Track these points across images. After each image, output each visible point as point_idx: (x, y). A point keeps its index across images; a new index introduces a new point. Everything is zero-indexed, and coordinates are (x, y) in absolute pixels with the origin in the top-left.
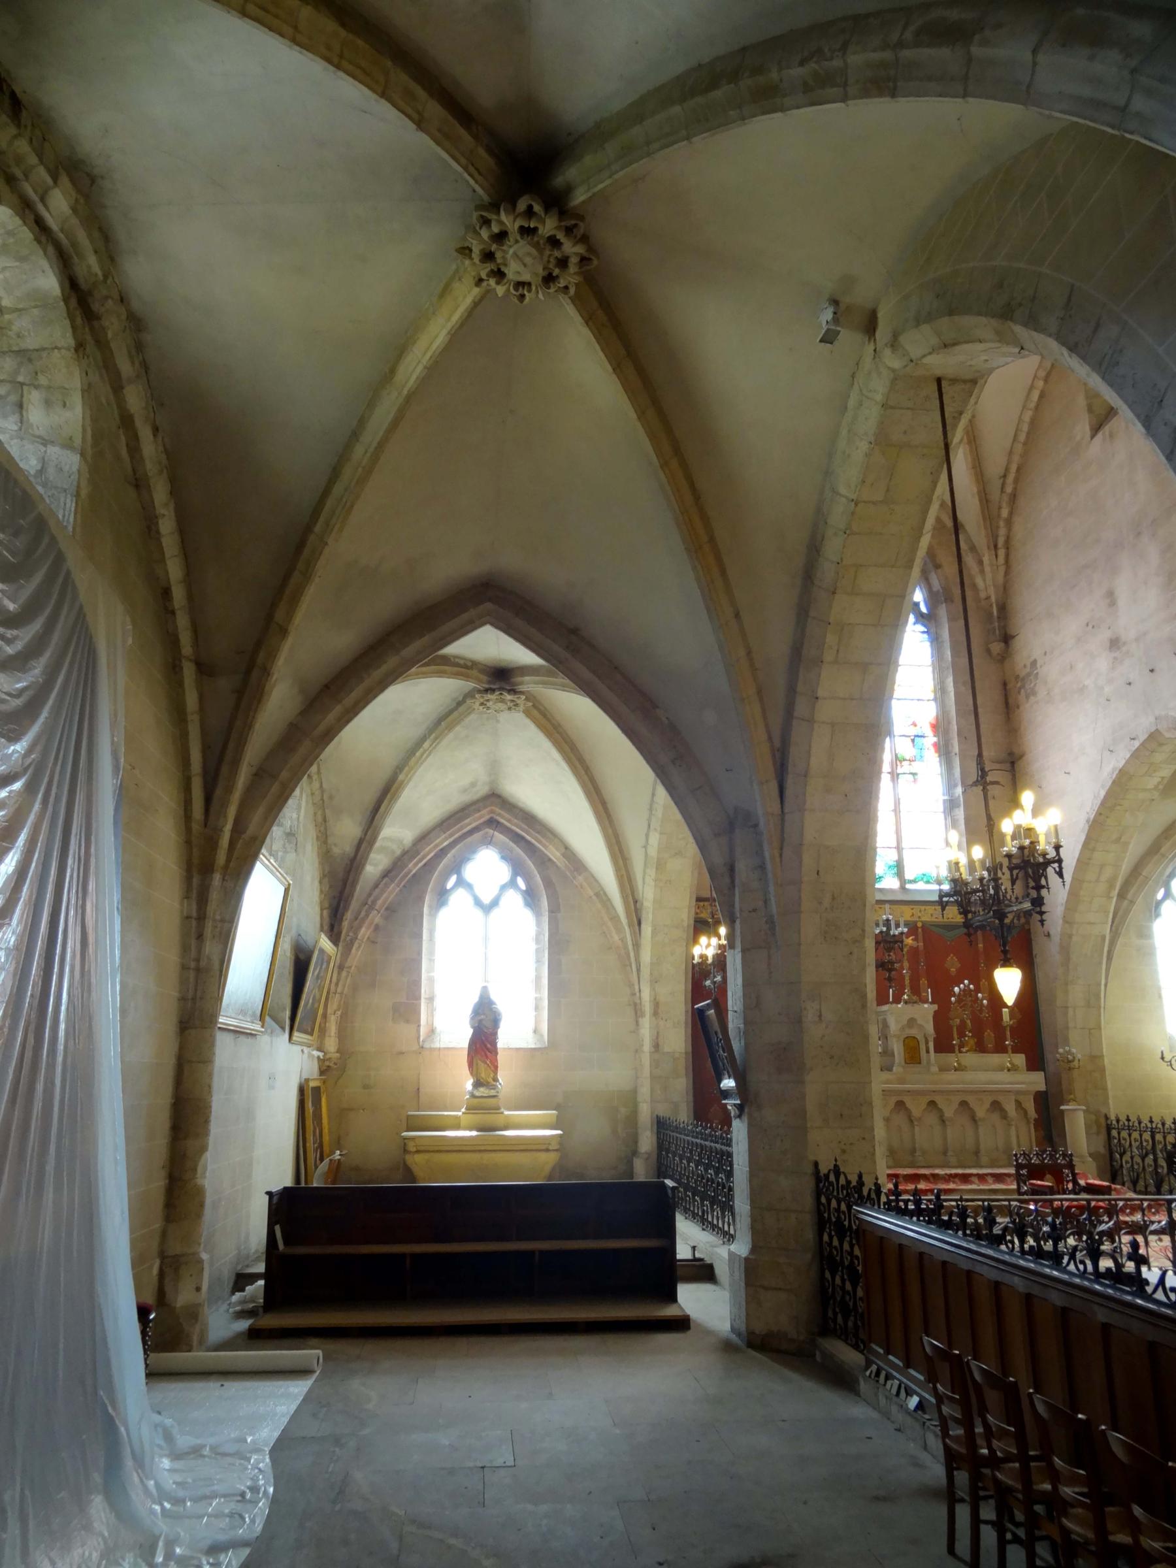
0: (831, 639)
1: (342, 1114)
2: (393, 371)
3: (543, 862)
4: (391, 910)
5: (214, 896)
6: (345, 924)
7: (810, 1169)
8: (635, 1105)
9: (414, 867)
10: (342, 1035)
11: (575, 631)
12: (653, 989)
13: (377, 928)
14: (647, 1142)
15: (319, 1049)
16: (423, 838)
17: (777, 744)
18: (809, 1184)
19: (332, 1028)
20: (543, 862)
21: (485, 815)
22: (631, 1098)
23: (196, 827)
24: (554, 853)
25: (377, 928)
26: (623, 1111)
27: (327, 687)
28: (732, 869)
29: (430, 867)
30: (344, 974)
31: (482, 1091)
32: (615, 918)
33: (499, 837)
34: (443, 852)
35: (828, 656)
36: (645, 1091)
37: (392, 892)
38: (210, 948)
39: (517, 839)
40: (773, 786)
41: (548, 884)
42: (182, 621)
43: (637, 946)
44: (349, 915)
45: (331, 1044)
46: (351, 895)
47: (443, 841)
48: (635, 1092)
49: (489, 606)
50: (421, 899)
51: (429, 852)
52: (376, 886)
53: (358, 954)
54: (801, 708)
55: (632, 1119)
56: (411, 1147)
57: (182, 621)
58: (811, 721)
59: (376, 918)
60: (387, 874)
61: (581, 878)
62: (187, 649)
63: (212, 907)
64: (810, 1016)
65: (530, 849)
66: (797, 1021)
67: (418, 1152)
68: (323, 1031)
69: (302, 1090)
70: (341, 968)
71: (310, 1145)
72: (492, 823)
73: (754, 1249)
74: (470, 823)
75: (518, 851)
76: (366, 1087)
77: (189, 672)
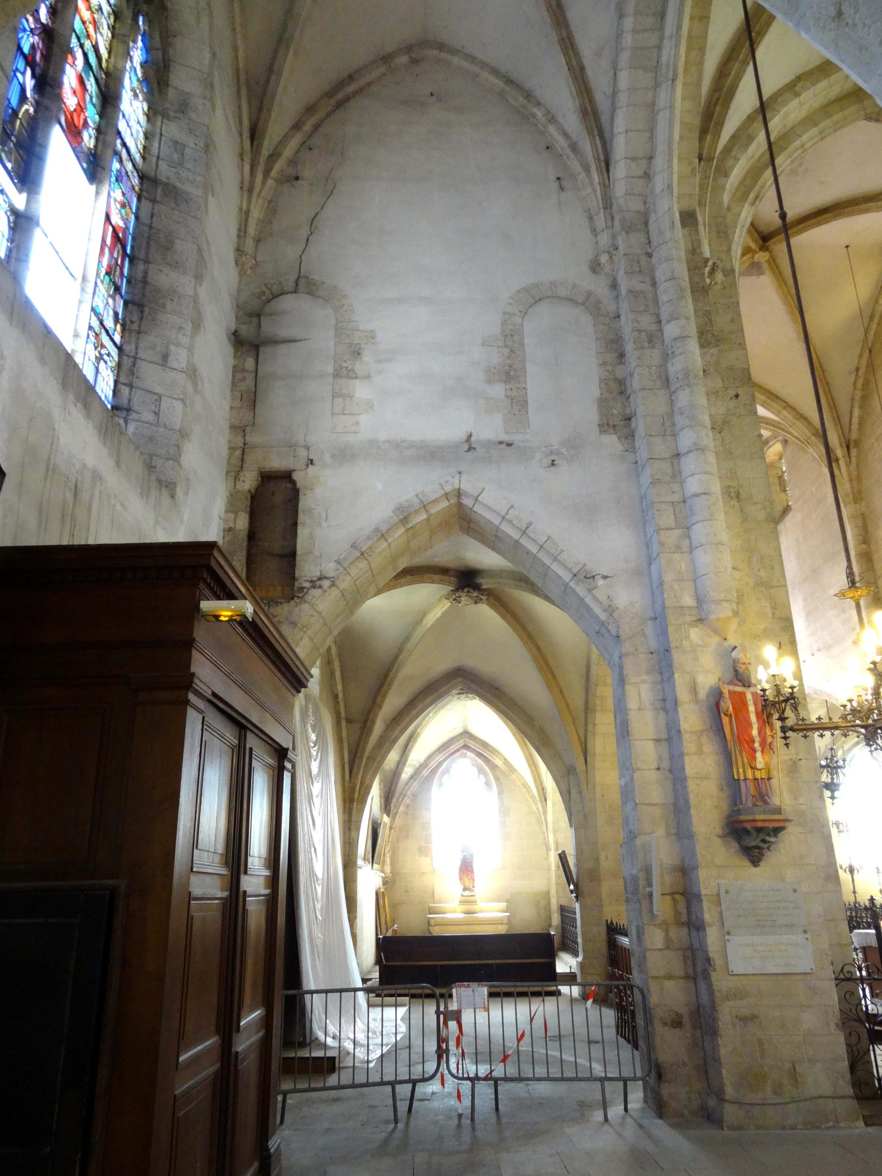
0: (598, 702)
1: (394, 906)
2: (422, 620)
3: (493, 767)
4: (415, 796)
5: (354, 812)
6: (392, 805)
7: (605, 923)
8: (549, 899)
9: (425, 773)
10: (392, 865)
11: (497, 689)
12: (555, 835)
13: (408, 806)
14: (556, 920)
15: (382, 872)
16: (430, 757)
17: (583, 740)
18: (604, 929)
19: (388, 861)
20: (493, 767)
21: (461, 743)
23: (347, 784)
24: (498, 762)
25: (408, 806)
26: (543, 903)
27: (394, 719)
28: (570, 793)
29: (434, 771)
30: (392, 831)
31: (467, 893)
32: (533, 797)
33: (469, 754)
34: (441, 763)
35: (598, 708)
36: (553, 891)
37: (415, 785)
38: (353, 834)
39: (479, 755)
40: (583, 758)
41: (497, 779)
42: (342, 705)
43: (545, 813)
44: (394, 800)
45: (388, 869)
46: (396, 788)
47: (439, 758)
48: (548, 893)
49: (460, 679)
50: (429, 789)
51: (433, 764)
52: (407, 784)
53: (398, 821)
54: (590, 728)
56: (432, 922)
57: (342, 705)
58: (594, 734)
59: (407, 801)
60: (412, 777)
61: (514, 776)
62: (343, 715)
63: (354, 818)
64: (602, 857)
65: (487, 761)
66: (597, 859)
67: (436, 925)
68: (384, 862)
69: (377, 894)
70: (391, 828)
71: (383, 922)
72: (466, 747)
73: (583, 959)
74: (453, 748)
75: (480, 761)
76: (407, 891)
77: (344, 723)
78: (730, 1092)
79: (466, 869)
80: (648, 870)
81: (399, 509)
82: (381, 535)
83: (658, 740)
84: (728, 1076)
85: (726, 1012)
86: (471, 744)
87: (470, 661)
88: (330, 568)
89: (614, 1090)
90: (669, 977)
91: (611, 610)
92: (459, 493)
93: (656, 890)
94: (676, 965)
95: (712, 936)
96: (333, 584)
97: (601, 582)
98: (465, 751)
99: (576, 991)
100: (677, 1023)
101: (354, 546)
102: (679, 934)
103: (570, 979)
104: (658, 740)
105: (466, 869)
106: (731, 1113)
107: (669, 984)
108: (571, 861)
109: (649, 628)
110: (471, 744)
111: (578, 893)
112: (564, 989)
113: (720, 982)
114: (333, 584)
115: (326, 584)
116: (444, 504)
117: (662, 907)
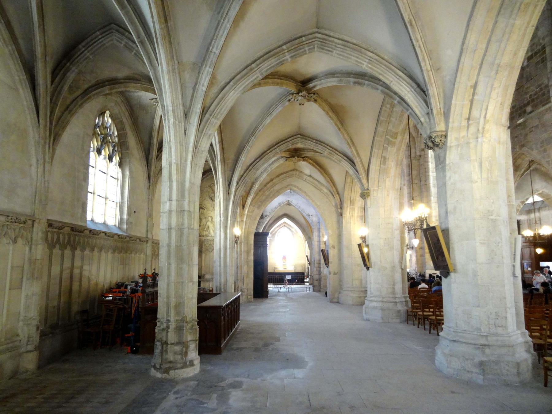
3: (292, 231)
8: (305, 265)
14: (307, 271)
20: (292, 231)
21: (283, 225)
22: (305, 265)
26: (304, 266)
29: (276, 232)
31: (284, 264)
34: (277, 230)
39: (288, 228)
43: (305, 244)
47: (277, 229)
55: (305, 268)
56: (275, 270)
65: (290, 229)
72: (285, 226)
74: (281, 226)
78: (322, 288)
79: (284, 258)
80: (314, 260)
81: (279, 204)
82: (276, 208)
83: (318, 242)
84: (322, 286)
85: (323, 278)
86: (286, 225)
87: (287, 213)
88: (268, 213)
89: (308, 289)
90: (317, 274)
91: (312, 221)
92: (289, 201)
93: (315, 263)
94: (318, 273)
95: (322, 269)
96: (269, 216)
97: (311, 216)
98: (284, 227)
99: (308, 284)
100: (317, 280)
101: (272, 210)
102: (318, 269)
103: (307, 282)
104: (318, 242)
105: (284, 258)
106: (322, 290)
107: (317, 275)
108: (309, 257)
109: (318, 224)
110: (286, 225)
111: (310, 264)
112: (306, 284)
113: (322, 274)
114: (269, 216)
115: (267, 216)
116: (286, 202)
117: (316, 265)
